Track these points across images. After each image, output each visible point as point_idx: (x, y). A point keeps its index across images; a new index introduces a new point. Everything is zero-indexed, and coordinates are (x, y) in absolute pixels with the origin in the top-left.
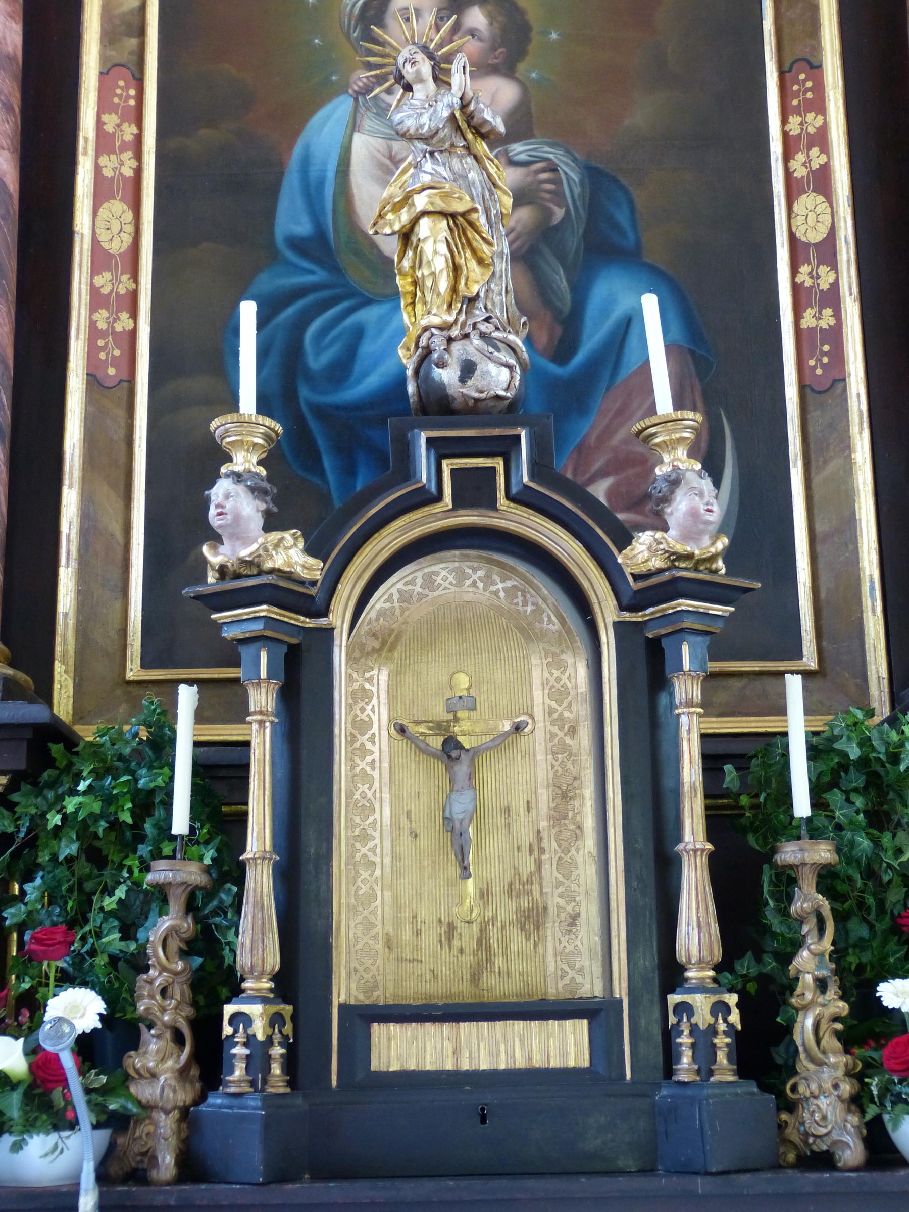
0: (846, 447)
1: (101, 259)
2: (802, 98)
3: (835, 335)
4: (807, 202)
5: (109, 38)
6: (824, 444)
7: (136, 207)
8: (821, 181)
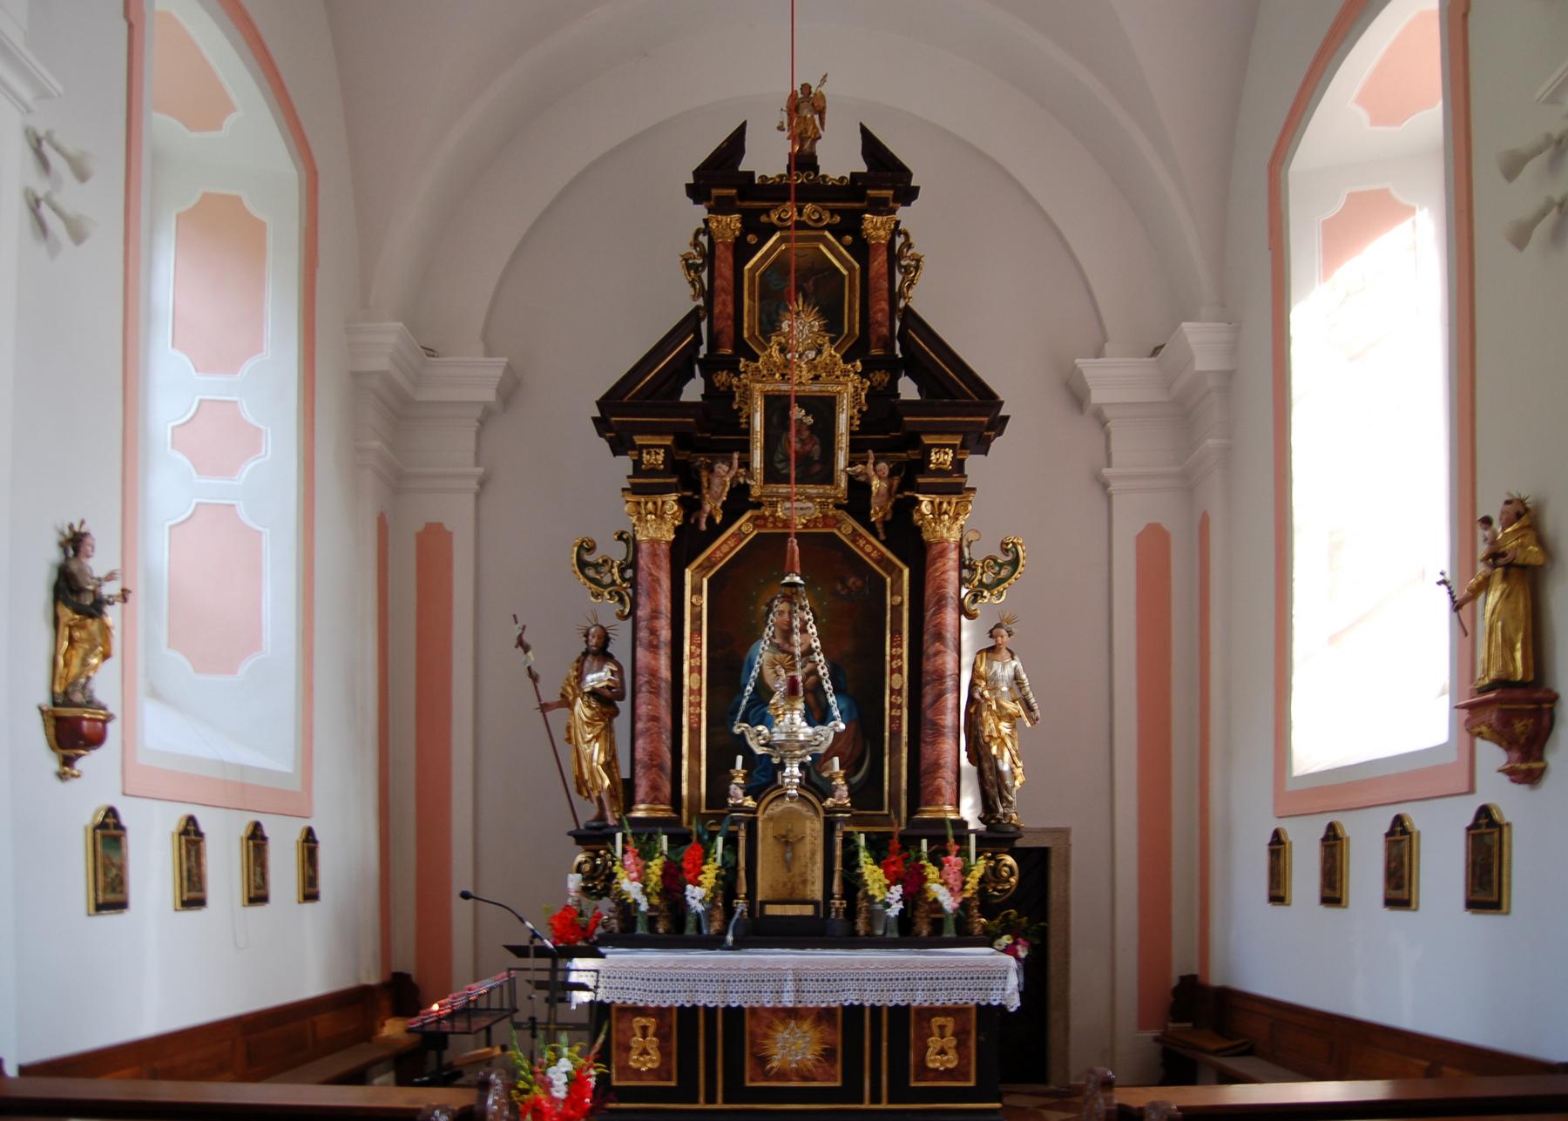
0: (900, 751)
1: (691, 692)
2: (896, 644)
3: (900, 718)
4: (896, 676)
5: (692, 622)
6: (895, 750)
7: (700, 674)
8: (900, 670)
